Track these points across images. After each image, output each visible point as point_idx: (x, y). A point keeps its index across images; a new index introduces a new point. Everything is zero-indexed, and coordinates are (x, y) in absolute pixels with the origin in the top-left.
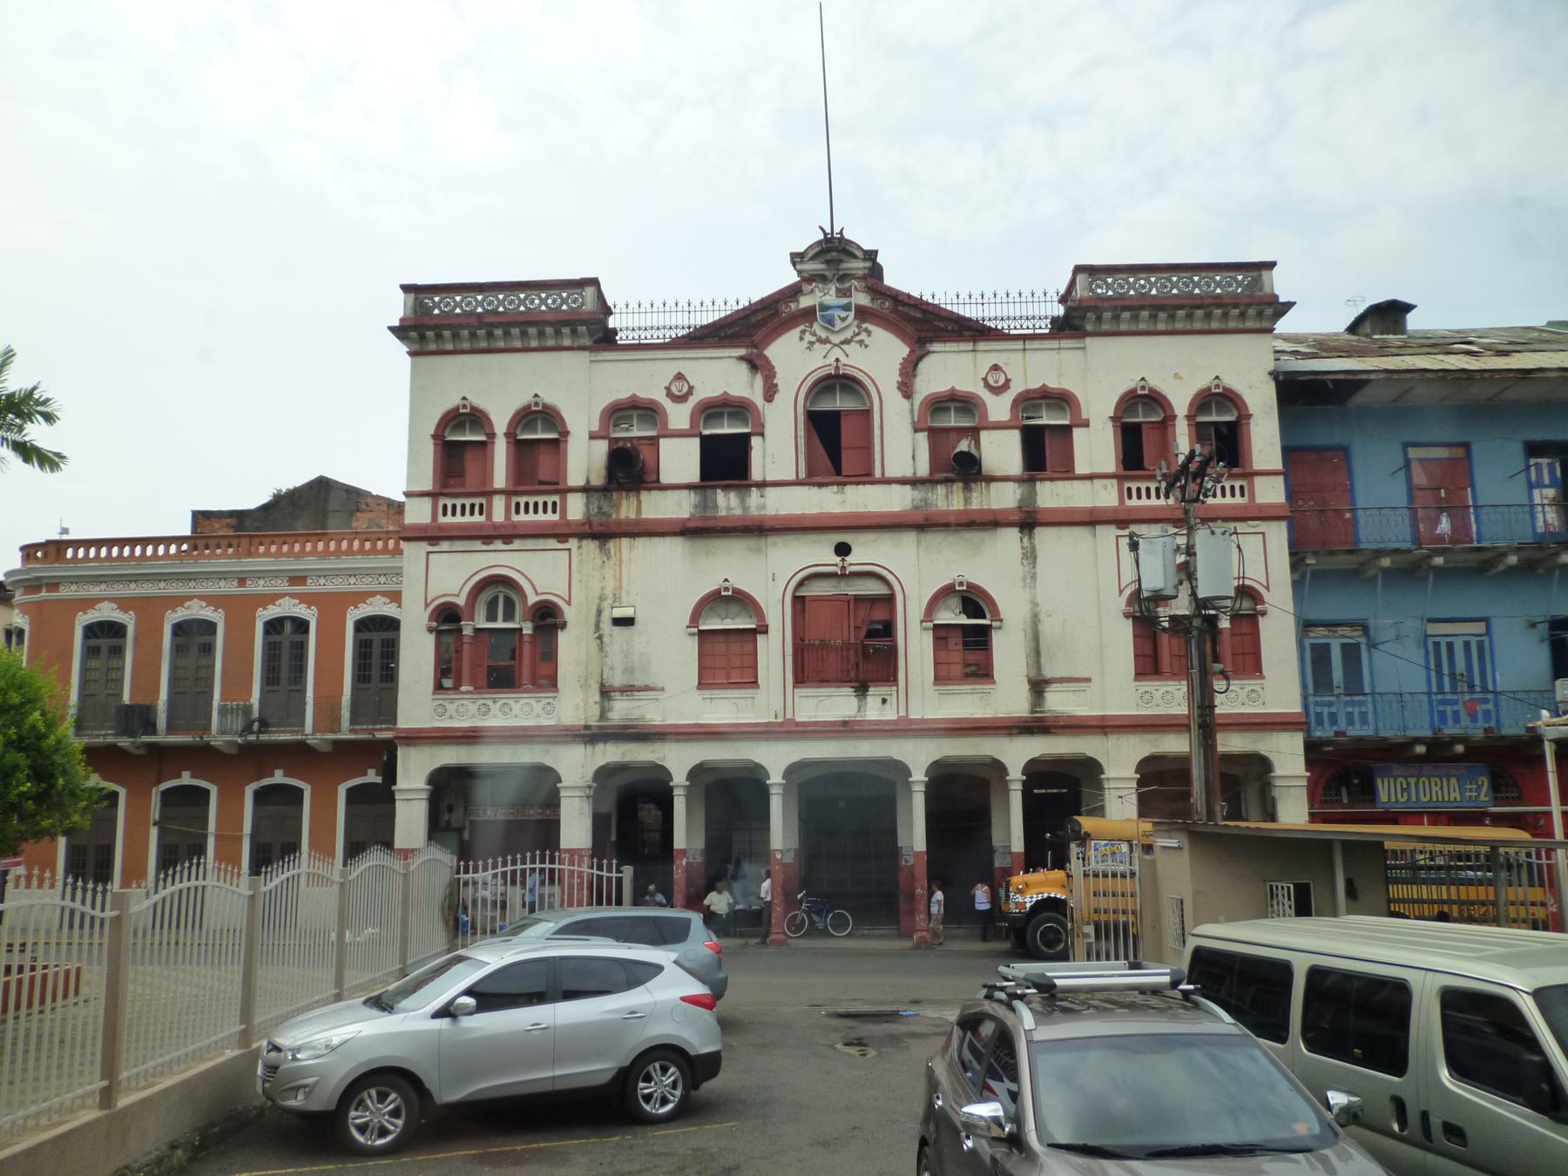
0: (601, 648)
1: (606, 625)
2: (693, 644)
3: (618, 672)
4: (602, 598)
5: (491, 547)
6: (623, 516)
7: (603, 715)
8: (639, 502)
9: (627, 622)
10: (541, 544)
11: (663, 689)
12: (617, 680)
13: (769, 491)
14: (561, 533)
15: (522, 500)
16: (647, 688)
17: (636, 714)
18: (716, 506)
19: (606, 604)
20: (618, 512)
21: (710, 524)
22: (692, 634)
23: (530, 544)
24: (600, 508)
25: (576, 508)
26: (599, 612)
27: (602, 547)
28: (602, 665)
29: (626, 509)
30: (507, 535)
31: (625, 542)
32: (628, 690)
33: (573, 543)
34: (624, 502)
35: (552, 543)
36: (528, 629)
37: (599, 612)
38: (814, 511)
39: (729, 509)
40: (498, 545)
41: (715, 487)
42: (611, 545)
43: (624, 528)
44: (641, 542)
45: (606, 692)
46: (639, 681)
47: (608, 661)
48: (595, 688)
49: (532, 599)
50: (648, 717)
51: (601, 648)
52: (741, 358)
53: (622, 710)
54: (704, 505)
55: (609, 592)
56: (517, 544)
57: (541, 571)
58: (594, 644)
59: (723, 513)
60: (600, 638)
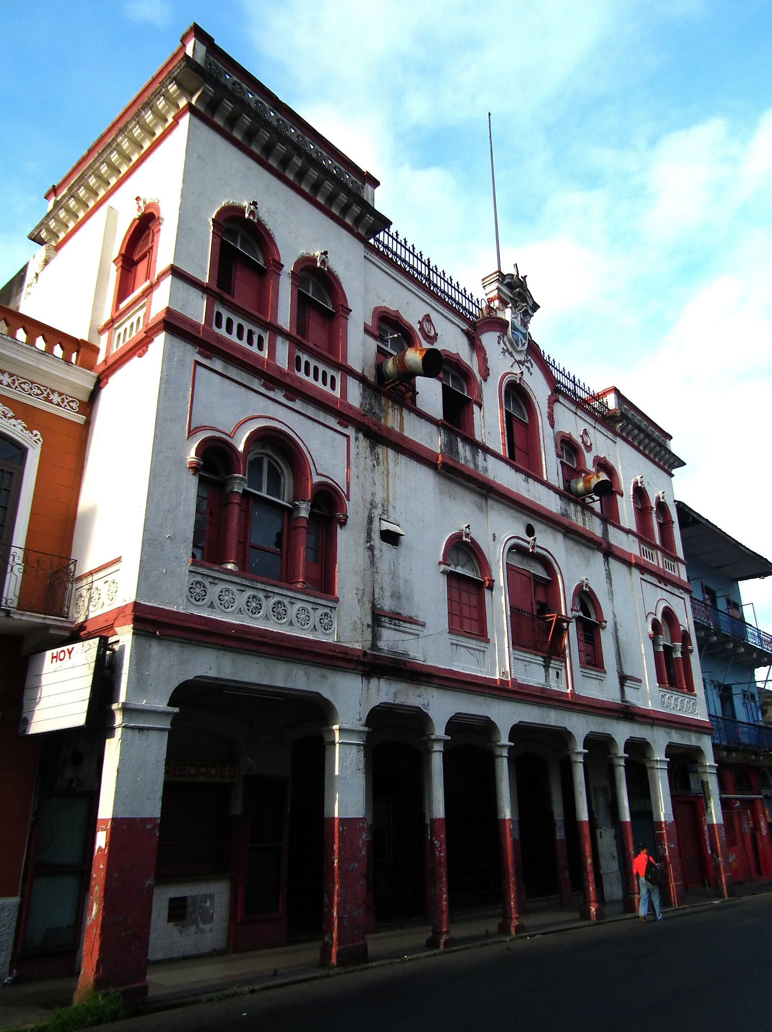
0: (372, 560)
1: (376, 536)
2: (443, 581)
3: (387, 594)
4: (373, 505)
5: (271, 394)
6: (390, 425)
7: (374, 646)
8: (402, 418)
9: (391, 538)
10: (322, 417)
11: (423, 625)
12: (387, 604)
13: (489, 457)
14: (344, 416)
15: (304, 358)
16: (411, 621)
17: (401, 649)
18: (458, 453)
19: (377, 512)
20: (386, 419)
21: (457, 466)
22: (443, 572)
23: (311, 411)
24: (371, 407)
25: (355, 395)
26: (370, 520)
27: (372, 448)
28: (374, 582)
29: (393, 419)
30: (295, 392)
31: (391, 452)
32: (398, 619)
33: (350, 431)
34: (390, 410)
35: (332, 422)
36: (304, 512)
37: (370, 520)
38: (515, 490)
39: (465, 457)
40: (279, 395)
41: (457, 434)
42: (380, 450)
43: (392, 438)
44: (403, 460)
45: (378, 618)
46: (405, 612)
47: (378, 578)
48: (368, 606)
49: (316, 479)
50: (412, 654)
51: (372, 560)
52: (466, 333)
53: (391, 640)
54: (450, 447)
55: (378, 499)
56: (298, 405)
57: (329, 452)
58: (367, 554)
59: (462, 462)
60: (371, 549)
